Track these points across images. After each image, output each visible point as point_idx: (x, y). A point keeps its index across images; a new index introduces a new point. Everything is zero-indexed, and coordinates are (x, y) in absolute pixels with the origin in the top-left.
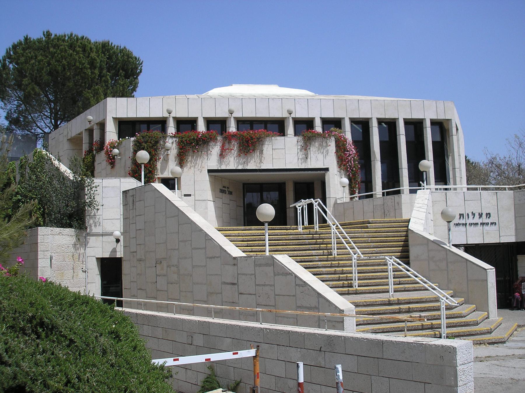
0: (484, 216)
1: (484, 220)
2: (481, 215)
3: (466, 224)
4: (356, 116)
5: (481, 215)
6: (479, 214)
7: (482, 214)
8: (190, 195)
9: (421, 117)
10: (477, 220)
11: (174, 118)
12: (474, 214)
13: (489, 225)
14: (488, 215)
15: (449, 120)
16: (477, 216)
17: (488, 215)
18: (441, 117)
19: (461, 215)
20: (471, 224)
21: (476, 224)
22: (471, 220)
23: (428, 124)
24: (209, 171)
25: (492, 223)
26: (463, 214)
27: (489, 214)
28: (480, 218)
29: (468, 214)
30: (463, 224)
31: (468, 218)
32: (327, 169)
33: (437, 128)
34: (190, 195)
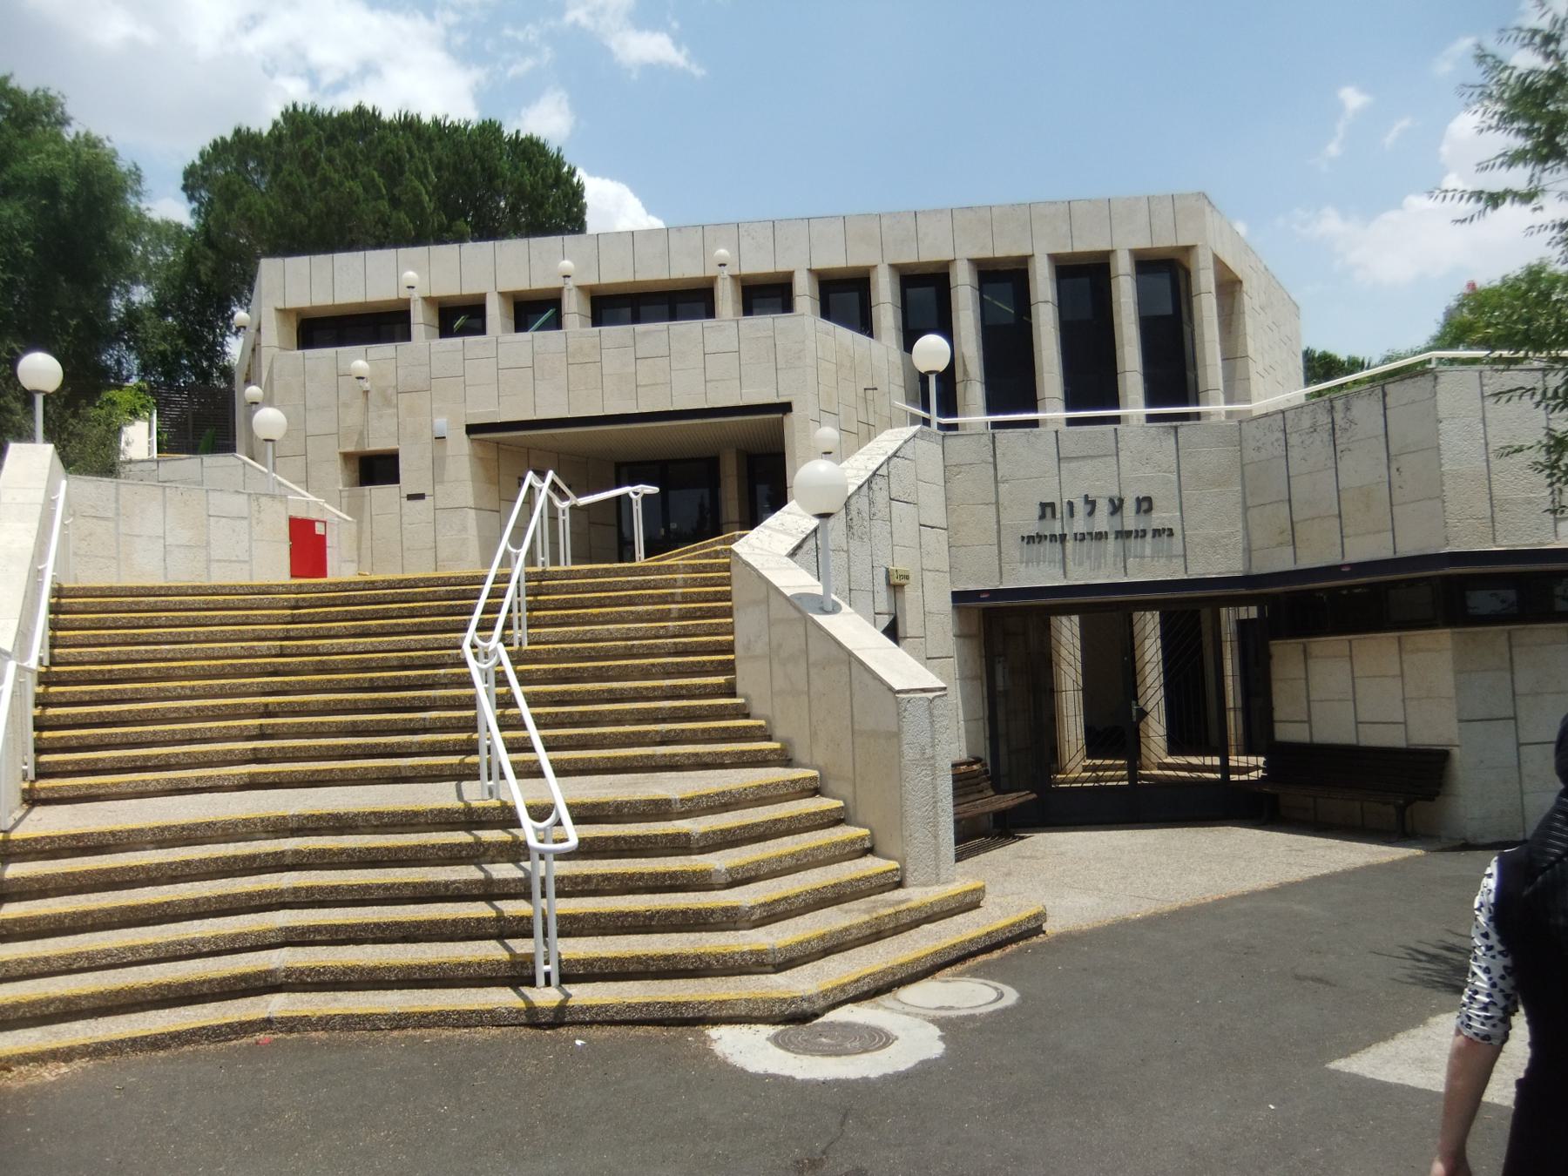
0: (1129, 507)
1: (1130, 520)
2: (1116, 507)
3: (1063, 537)
4: (908, 257)
5: (1116, 507)
6: (1111, 501)
7: (1121, 501)
8: (421, 496)
9: (1102, 246)
10: (1102, 521)
11: (428, 300)
12: (1091, 504)
13: (1149, 535)
14: (1145, 505)
15: (1188, 250)
16: (1103, 508)
17: (1145, 505)
18: (1165, 240)
19: (1047, 509)
20: (1081, 538)
21: (1100, 536)
22: (1080, 525)
23: (1123, 267)
24: (471, 429)
25: (1157, 533)
26: (1052, 505)
27: (1148, 499)
28: (1113, 513)
29: (1071, 504)
30: (1053, 537)
31: (1072, 514)
32: (786, 408)
33: (1163, 283)
34: (421, 496)
